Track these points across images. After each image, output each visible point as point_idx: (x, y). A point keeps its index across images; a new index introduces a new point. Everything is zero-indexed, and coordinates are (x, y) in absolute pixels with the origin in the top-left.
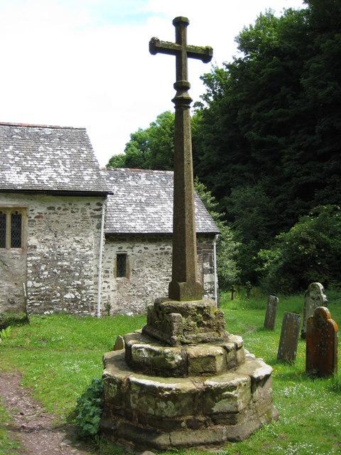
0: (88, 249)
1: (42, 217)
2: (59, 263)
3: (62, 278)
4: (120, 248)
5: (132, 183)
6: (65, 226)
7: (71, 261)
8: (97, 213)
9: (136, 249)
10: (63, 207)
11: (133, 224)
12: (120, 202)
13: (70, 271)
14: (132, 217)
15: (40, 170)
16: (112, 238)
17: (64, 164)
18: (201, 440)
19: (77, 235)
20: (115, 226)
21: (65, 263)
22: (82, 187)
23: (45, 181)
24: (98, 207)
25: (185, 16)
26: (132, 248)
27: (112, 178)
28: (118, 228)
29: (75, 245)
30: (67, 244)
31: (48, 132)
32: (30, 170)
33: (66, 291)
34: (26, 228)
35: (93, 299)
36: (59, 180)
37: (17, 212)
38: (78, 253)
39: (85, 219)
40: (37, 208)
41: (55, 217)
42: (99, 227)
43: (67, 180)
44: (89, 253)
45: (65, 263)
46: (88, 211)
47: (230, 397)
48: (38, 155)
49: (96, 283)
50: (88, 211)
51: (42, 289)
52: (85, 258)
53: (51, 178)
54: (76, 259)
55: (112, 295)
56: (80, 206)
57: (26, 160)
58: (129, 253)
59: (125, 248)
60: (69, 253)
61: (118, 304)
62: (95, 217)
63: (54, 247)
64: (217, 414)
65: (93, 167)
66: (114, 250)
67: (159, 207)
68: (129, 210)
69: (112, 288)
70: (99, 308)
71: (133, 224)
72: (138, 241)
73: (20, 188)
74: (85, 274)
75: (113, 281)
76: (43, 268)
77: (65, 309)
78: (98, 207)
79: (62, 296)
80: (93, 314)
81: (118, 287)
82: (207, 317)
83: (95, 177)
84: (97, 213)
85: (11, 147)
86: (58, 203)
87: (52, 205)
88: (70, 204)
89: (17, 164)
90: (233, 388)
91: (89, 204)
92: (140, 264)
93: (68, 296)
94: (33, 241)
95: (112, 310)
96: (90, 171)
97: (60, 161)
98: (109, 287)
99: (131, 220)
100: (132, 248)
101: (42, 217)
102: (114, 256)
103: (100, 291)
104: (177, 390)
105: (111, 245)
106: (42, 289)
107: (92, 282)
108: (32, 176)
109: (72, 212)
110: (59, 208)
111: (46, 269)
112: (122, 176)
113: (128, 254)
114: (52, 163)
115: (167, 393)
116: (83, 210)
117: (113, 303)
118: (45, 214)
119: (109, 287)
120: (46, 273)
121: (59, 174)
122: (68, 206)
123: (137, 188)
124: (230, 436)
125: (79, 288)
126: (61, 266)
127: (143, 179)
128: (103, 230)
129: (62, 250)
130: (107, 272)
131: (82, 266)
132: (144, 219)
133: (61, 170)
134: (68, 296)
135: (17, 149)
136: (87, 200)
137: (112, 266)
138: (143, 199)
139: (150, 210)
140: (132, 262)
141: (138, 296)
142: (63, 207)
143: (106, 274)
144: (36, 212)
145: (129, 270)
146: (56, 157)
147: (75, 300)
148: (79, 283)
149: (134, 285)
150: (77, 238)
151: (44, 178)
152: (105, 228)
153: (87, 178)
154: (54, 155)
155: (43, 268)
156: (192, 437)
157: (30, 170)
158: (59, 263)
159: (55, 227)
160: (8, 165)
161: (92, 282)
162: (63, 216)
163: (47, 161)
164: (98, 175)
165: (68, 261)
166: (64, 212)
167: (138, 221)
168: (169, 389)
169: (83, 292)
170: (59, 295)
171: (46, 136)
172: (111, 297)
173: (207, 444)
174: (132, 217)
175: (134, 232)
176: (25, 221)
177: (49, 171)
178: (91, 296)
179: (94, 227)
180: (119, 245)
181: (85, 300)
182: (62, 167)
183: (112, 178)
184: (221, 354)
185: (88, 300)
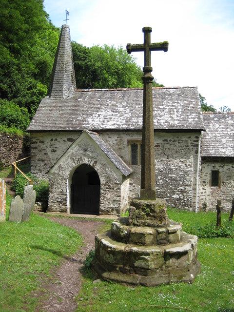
0: (189, 166)
1: (159, 146)
2: (170, 175)
3: (171, 185)
4: (215, 167)
6: (174, 151)
7: (178, 174)
8: (196, 143)
9: (226, 168)
10: (173, 140)
11: (224, 151)
12: (218, 135)
13: (177, 181)
14: (225, 145)
15: (161, 116)
16: (206, 160)
17: (177, 112)
18: (125, 280)
19: (182, 158)
20: (210, 152)
21: (174, 176)
22: (185, 127)
23: (162, 123)
24: (196, 139)
25: (147, 26)
26: (223, 167)
27: (216, 119)
28: (212, 153)
30: (175, 163)
31: (171, 91)
35: (191, 200)
37: (135, 144)
38: (182, 169)
39: (187, 147)
41: (167, 146)
42: (197, 152)
43: (176, 122)
44: (189, 169)
45: (174, 176)
46: (189, 142)
47: (144, 259)
48: (162, 107)
49: (195, 189)
50: (189, 142)
51: (158, 191)
52: (186, 173)
53: (166, 121)
54: (181, 173)
55: (208, 198)
56: (184, 139)
58: (220, 170)
59: (218, 166)
60: (176, 169)
61: (212, 204)
62: (195, 146)
63: (166, 165)
64: (137, 267)
65: (196, 113)
66: (209, 169)
68: (224, 140)
69: (208, 193)
70: (197, 206)
71: (224, 151)
72: (228, 162)
74: (187, 183)
75: (208, 189)
76: (159, 178)
77: (172, 205)
78: (196, 139)
79: (171, 196)
80: (191, 209)
81: (212, 193)
82: (153, 211)
83: (196, 119)
84: (196, 143)
86: (170, 137)
87: (166, 138)
88: (178, 138)
90: (147, 254)
91: (190, 137)
92: (228, 178)
93: (175, 196)
95: (207, 208)
96: (194, 115)
97: (175, 110)
98: (205, 192)
99: (223, 148)
100: (223, 167)
101: (159, 146)
102: (209, 172)
103: (197, 195)
104: (114, 249)
105: (208, 164)
106: (158, 191)
107: (191, 189)
109: (179, 143)
110: (170, 141)
111: (161, 179)
113: (220, 171)
114: (169, 112)
115: (110, 249)
116: (186, 141)
117: (208, 203)
118: (161, 144)
119: (205, 192)
120: (161, 181)
121: (172, 118)
122: (176, 139)
124: (142, 282)
125: (182, 192)
126: (171, 177)
128: (199, 154)
130: (204, 182)
131: (184, 178)
133: (174, 116)
134: (175, 196)
136: (188, 135)
137: (208, 178)
140: (222, 175)
141: (227, 200)
142: (173, 140)
143: (204, 184)
145: (220, 181)
146: (173, 108)
147: (179, 199)
148: (182, 188)
149: (224, 192)
150: (182, 160)
151: (162, 122)
152: (201, 153)
153: (190, 120)
154: (172, 106)
155: (159, 178)
156: (121, 277)
158: (170, 175)
159: (167, 152)
161: (191, 189)
162: (173, 146)
163: (167, 110)
164: (199, 118)
165: (175, 174)
166: (173, 143)
167: (229, 148)
168: (111, 248)
169: (185, 194)
170: (169, 195)
171: (170, 94)
172: (207, 199)
173: (128, 283)
174: (225, 145)
175: (224, 156)
178: (189, 198)
179: (193, 152)
180: (213, 165)
181: (186, 199)
182: (176, 114)
183: (216, 119)
184: (151, 234)
185: (188, 200)
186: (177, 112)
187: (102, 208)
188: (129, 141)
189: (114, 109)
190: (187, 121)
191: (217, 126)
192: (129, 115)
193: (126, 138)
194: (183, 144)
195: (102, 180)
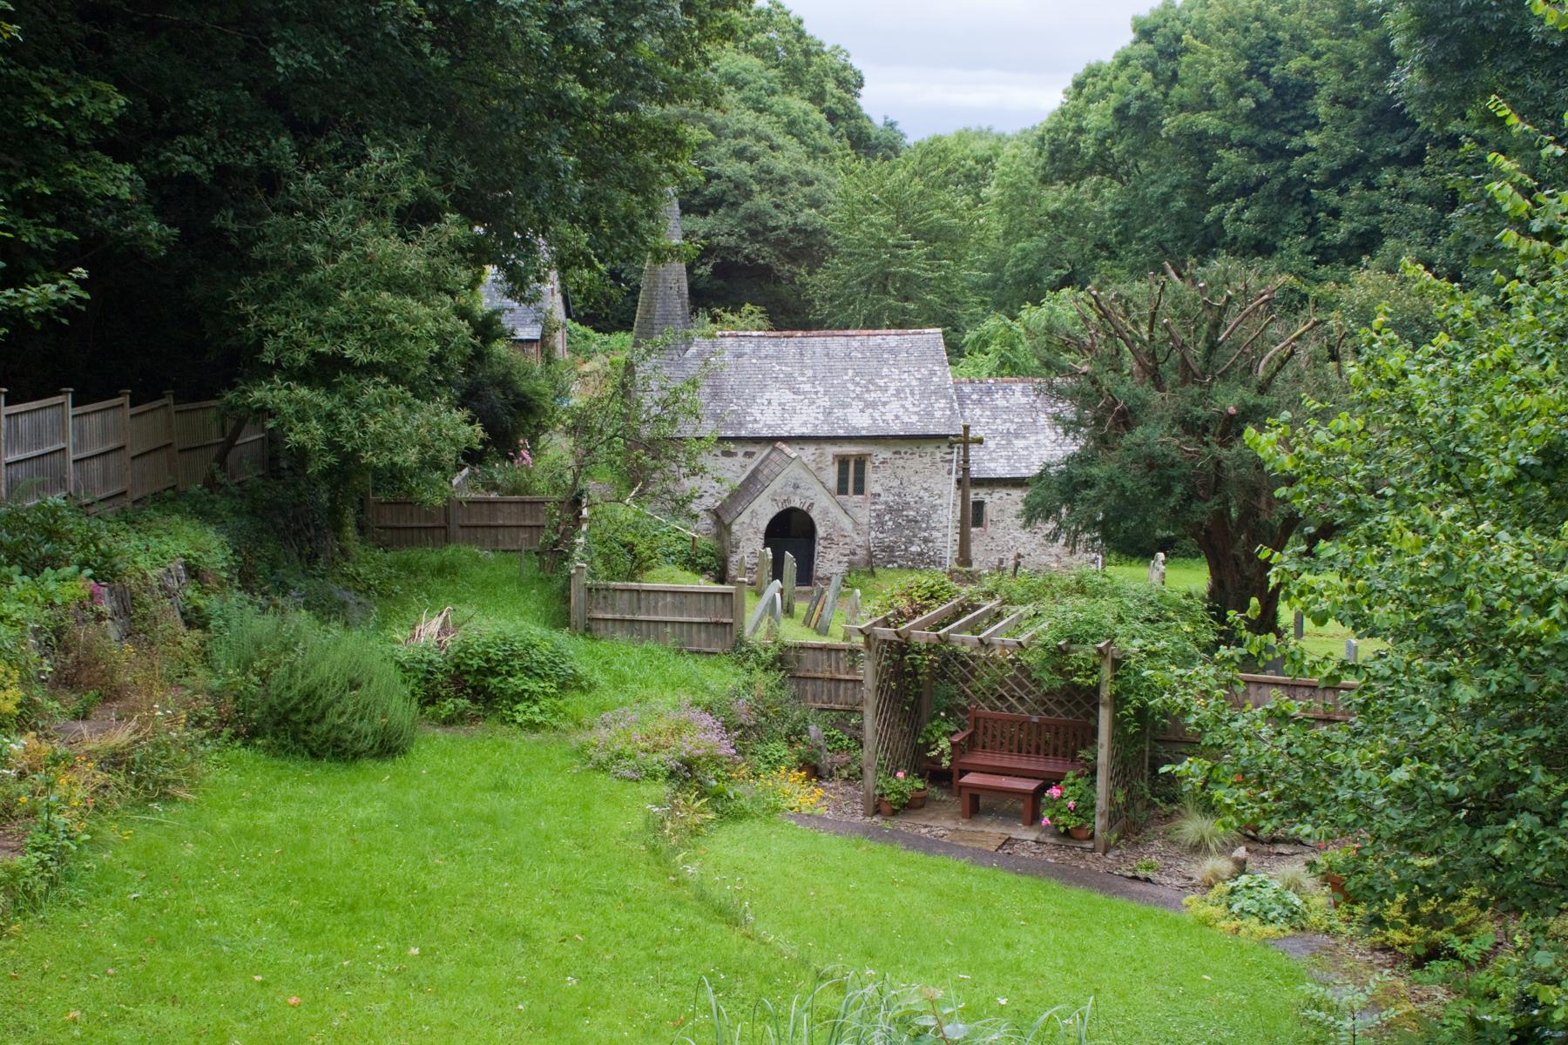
5: (1001, 403)
6: (912, 472)
9: (996, 496)
11: (992, 465)
15: (884, 404)
17: (912, 394)
29: (922, 493)
32: (873, 405)
33: (912, 543)
34: (870, 475)
36: (906, 420)
39: (934, 464)
40: (881, 454)
43: (915, 418)
46: (938, 455)
48: (881, 383)
49: (945, 535)
57: (868, 391)
58: (987, 499)
63: (899, 495)
65: (945, 397)
67: (1033, 439)
71: (992, 465)
73: (864, 433)
85: (850, 372)
89: (859, 397)
93: (913, 549)
94: (877, 489)
99: (991, 460)
108: (877, 415)
112: (989, 392)
121: (907, 410)
123: (1007, 410)
125: (926, 541)
127: (1018, 394)
129: (908, 499)
131: (929, 516)
132: (1009, 458)
133: (908, 404)
134: (913, 549)
135: (857, 374)
138: (1012, 428)
139: (1020, 443)
144: (880, 457)
147: (921, 554)
151: (889, 417)
153: (938, 414)
157: (873, 405)
160: (763, 124)
163: (892, 391)
164: (951, 409)
176: (869, 467)
177: (895, 406)
183: (975, 397)
186: (912, 394)
187: (820, 573)
188: (836, 456)
189: (790, 383)
190: (930, 415)
191: (978, 412)
192: (824, 401)
193: (832, 450)
194: (927, 459)
195: (821, 531)
